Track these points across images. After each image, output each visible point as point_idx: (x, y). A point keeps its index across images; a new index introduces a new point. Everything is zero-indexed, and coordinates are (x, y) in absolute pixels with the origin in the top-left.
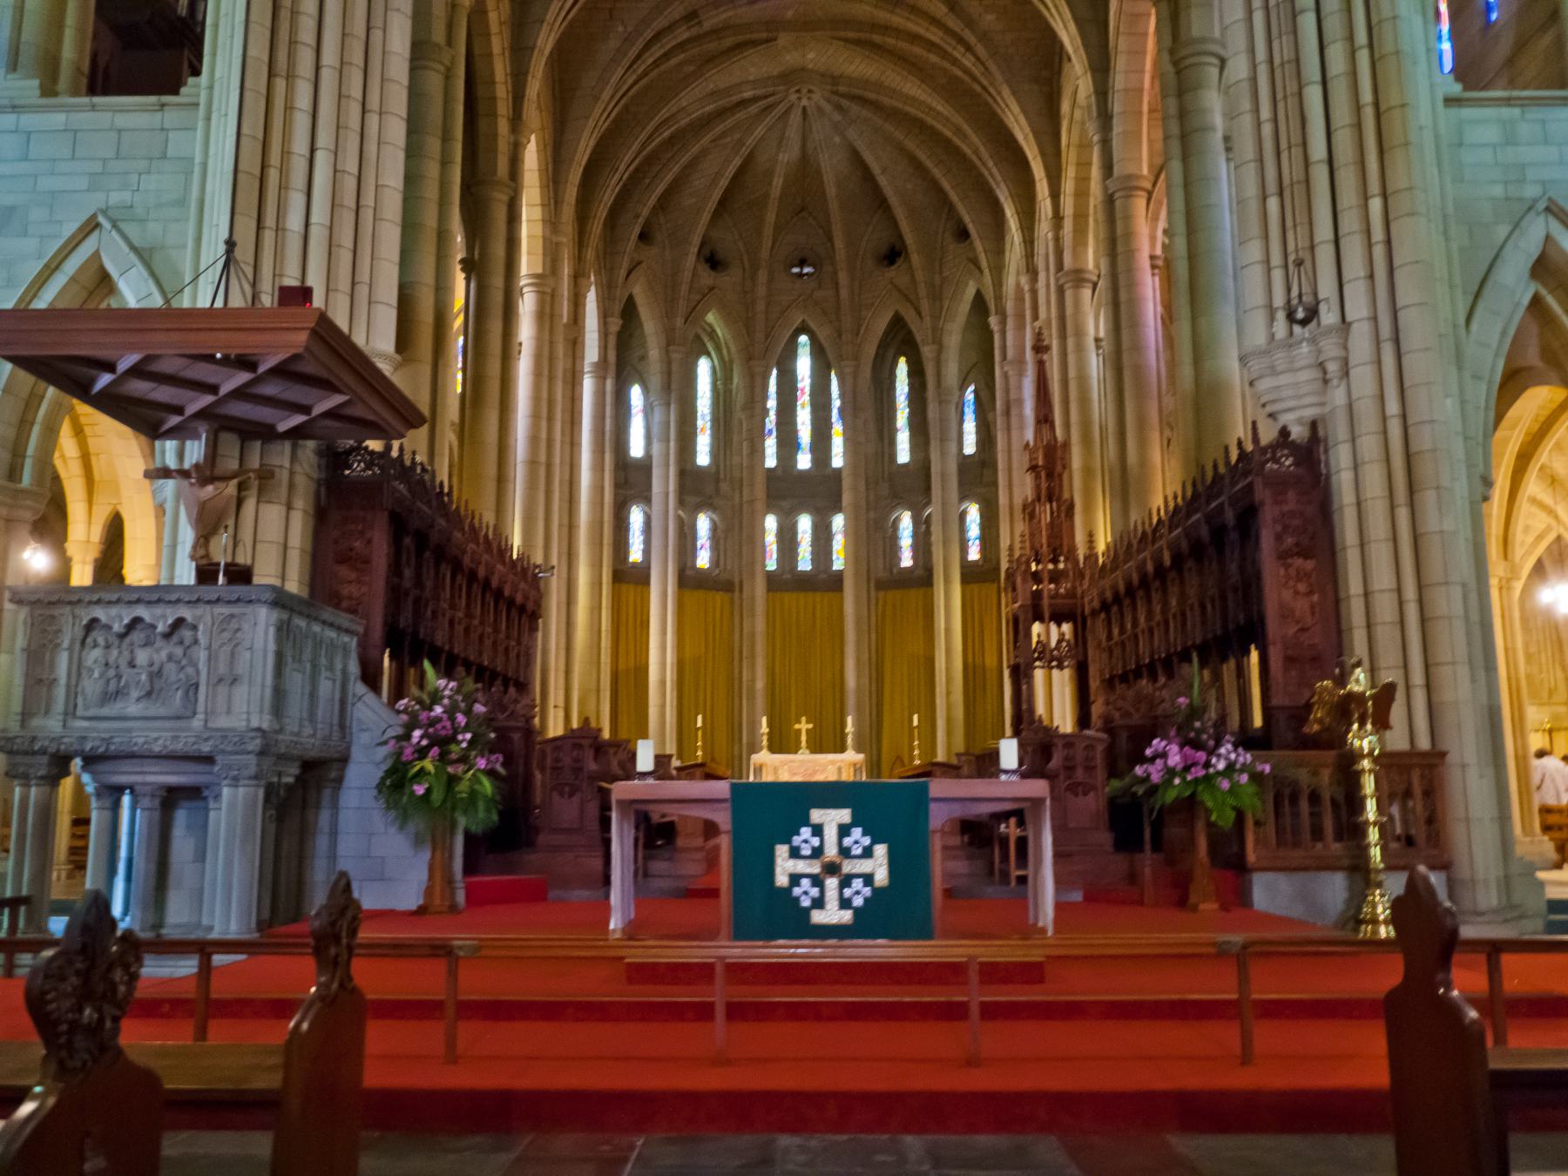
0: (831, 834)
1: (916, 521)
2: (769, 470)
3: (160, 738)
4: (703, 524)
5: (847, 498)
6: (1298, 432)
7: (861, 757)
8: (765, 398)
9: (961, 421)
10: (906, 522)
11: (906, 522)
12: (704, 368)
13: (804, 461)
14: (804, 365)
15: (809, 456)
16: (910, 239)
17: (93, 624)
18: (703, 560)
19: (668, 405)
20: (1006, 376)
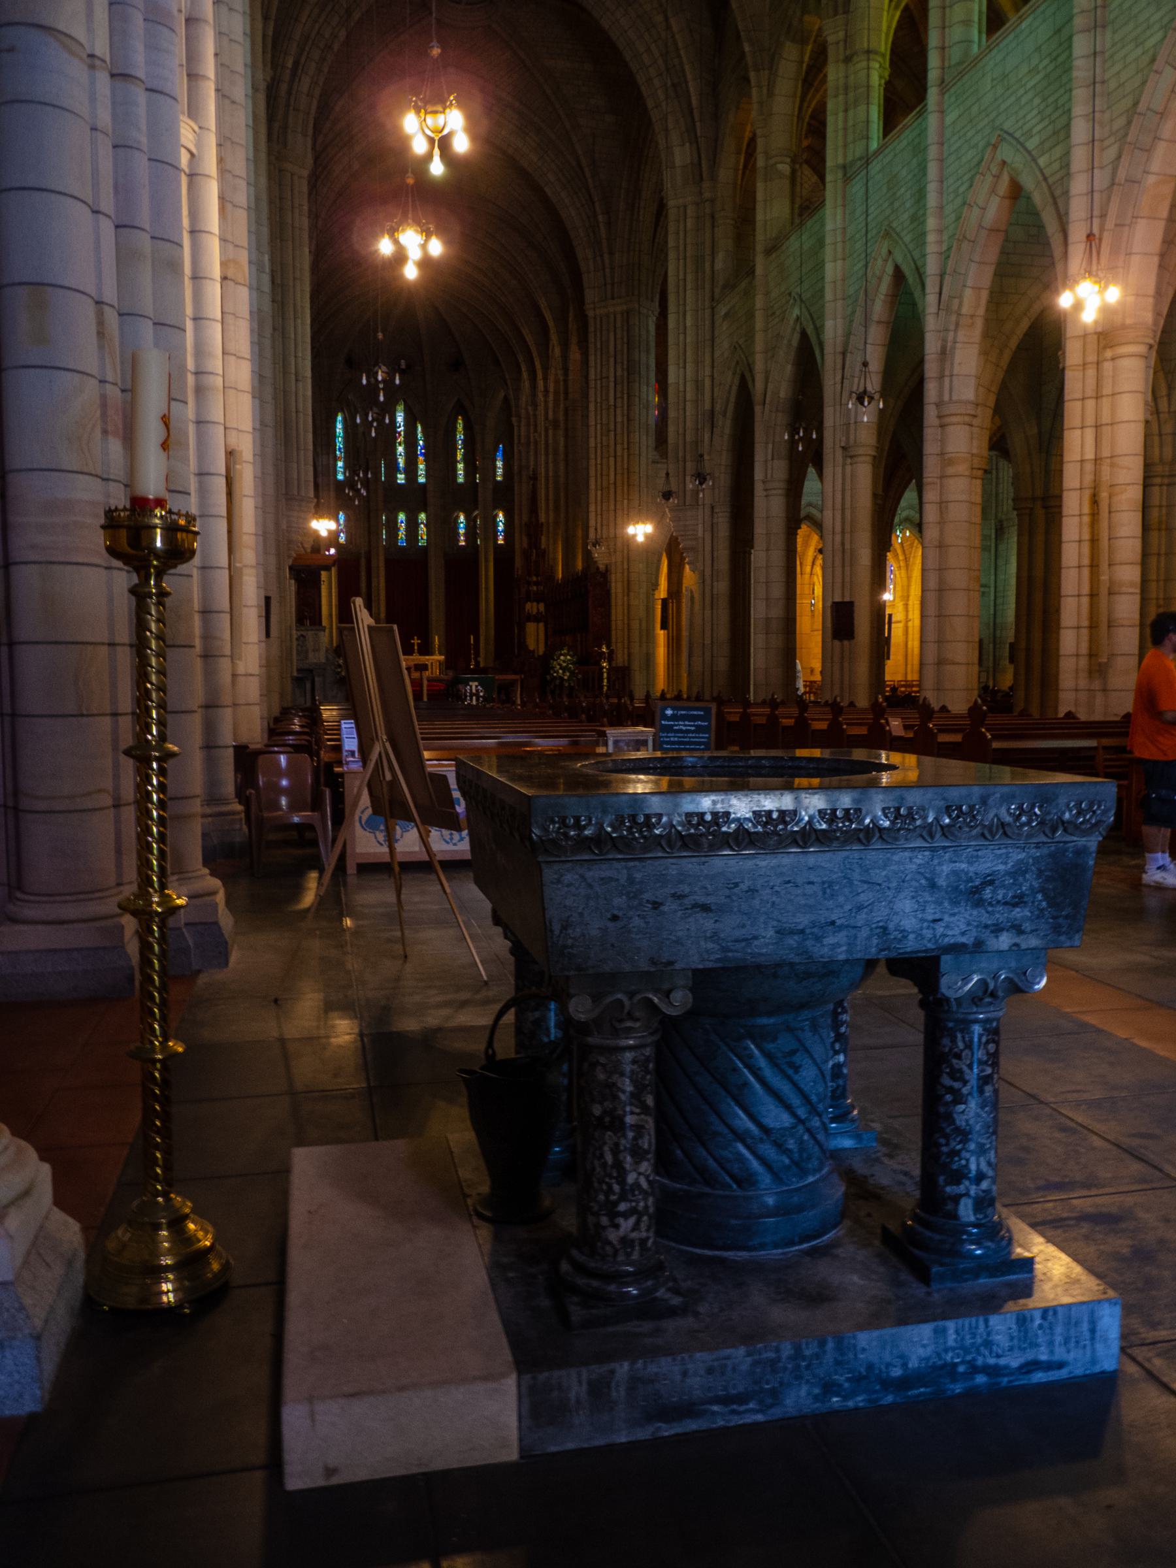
0: (474, 688)
1: (466, 518)
6: (602, 567)
7: (443, 657)
9: (495, 460)
10: (462, 518)
11: (462, 518)
12: (339, 418)
13: (401, 478)
14: (400, 418)
15: (403, 476)
20: (520, 452)
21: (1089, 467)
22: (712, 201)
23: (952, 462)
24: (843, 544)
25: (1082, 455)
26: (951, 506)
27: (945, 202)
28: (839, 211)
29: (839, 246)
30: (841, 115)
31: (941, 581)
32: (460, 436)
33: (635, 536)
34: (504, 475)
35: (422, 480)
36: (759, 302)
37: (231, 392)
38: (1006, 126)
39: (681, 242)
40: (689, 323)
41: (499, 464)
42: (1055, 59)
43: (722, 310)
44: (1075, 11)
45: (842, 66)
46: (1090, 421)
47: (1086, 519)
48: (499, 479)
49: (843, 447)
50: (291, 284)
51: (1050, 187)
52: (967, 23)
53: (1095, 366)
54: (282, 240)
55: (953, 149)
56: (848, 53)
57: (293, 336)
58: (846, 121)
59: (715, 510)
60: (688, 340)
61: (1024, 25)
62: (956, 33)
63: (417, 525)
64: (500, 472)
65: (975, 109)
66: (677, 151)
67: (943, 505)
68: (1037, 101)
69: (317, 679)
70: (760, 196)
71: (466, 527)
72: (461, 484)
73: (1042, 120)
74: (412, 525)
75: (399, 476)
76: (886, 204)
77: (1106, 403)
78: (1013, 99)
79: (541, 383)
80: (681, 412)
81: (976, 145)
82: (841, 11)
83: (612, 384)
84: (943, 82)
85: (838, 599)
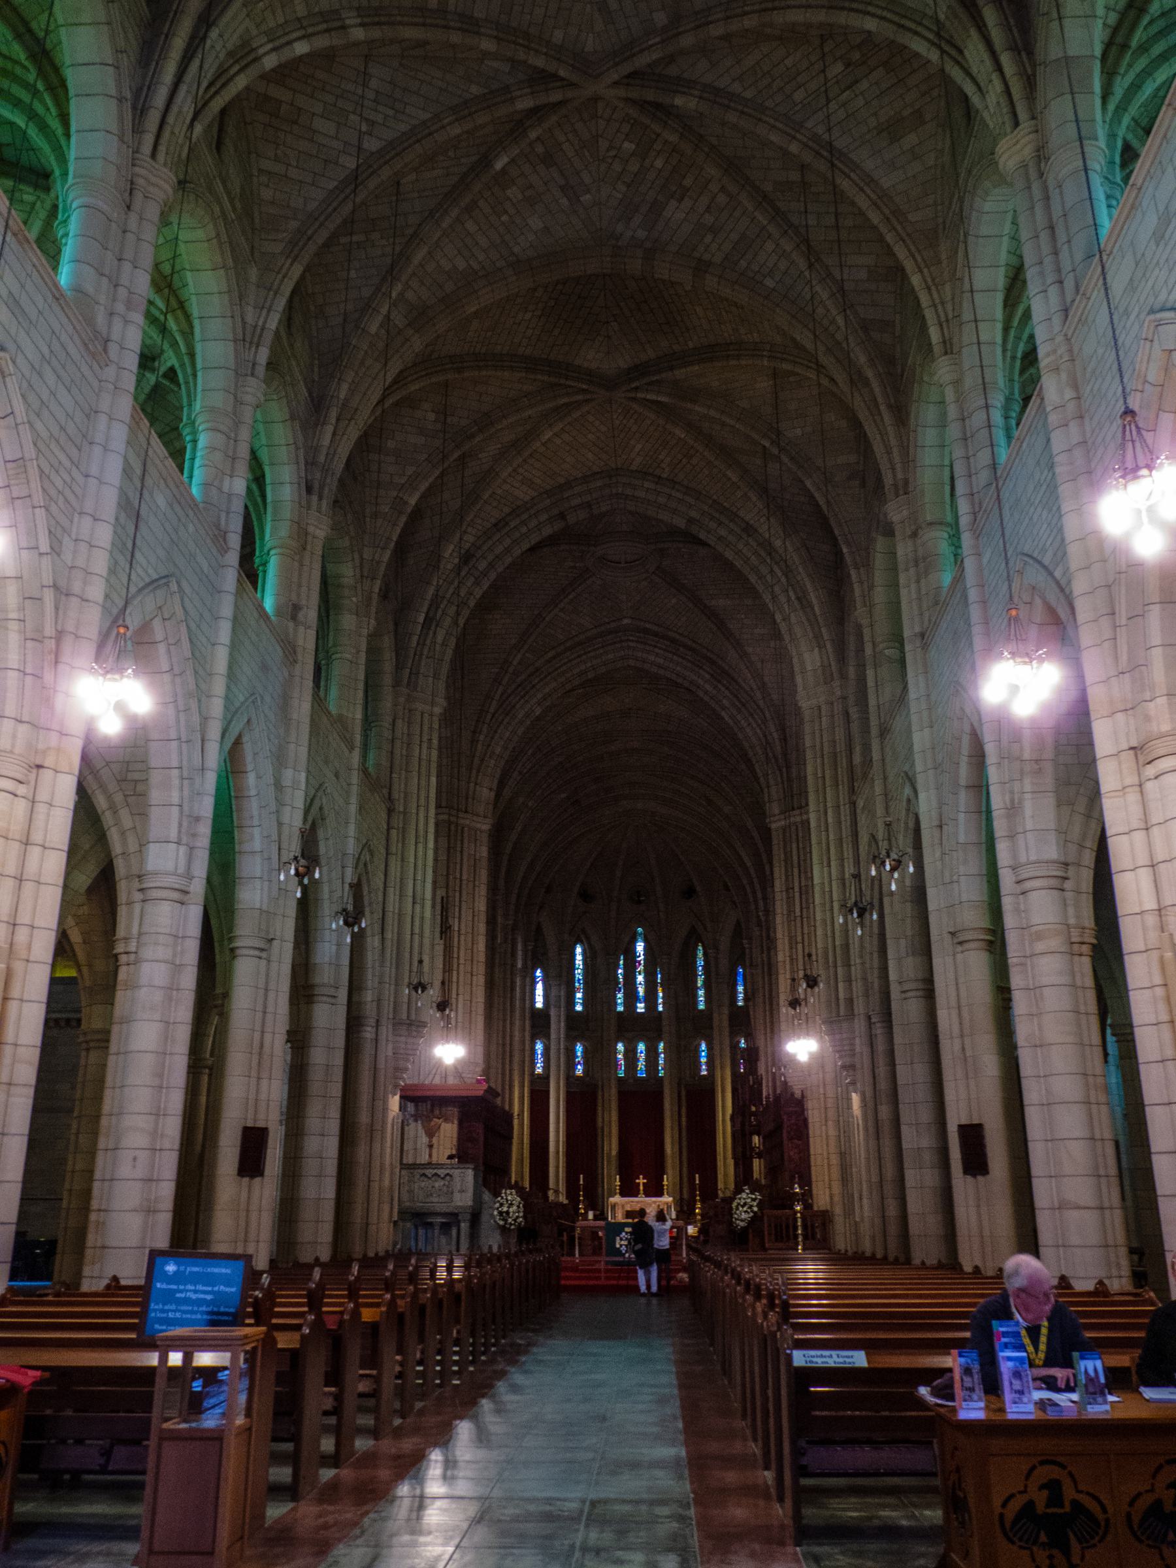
2: (620, 1013)
3: (444, 1208)
4: (579, 1049)
5: (665, 1029)
6: (798, 1094)
8: (618, 967)
9: (735, 985)
10: (703, 1047)
11: (703, 1047)
12: (579, 950)
13: (641, 1007)
14: (640, 947)
15: (642, 1005)
16: (698, 889)
17: (424, 1175)
18: (579, 1070)
19: (560, 985)
21: (1151, 920)
22: (844, 698)
23: (1039, 937)
24: (963, 1049)
25: (1141, 904)
26: (1046, 991)
28: (921, 678)
29: (925, 714)
30: (913, 586)
32: (700, 962)
34: (746, 999)
35: (660, 1008)
36: (878, 789)
37: (28, 887)
38: (1026, 549)
39: (818, 740)
40: (830, 820)
41: (740, 989)
43: (860, 803)
44: (1048, 409)
45: (910, 543)
46: (1143, 859)
47: (1160, 991)
48: (740, 1004)
49: (953, 934)
50: (414, 811)
53: (1138, 789)
54: (407, 771)
56: (913, 527)
57: (412, 860)
58: (919, 590)
59: (873, 1020)
60: (832, 837)
61: (1025, 445)
63: (657, 1054)
64: (741, 996)
66: (806, 656)
67: (1034, 989)
68: (1045, 512)
69: (463, 1225)
70: (870, 683)
71: (709, 1056)
72: (702, 1011)
74: (652, 1054)
75: (639, 1005)
77: (1155, 831)
78: (1027, 520)
79: (761, 903)
80: (828, 914)
82: (901, 492)
83: (797, 895)
85: (964, 1122)
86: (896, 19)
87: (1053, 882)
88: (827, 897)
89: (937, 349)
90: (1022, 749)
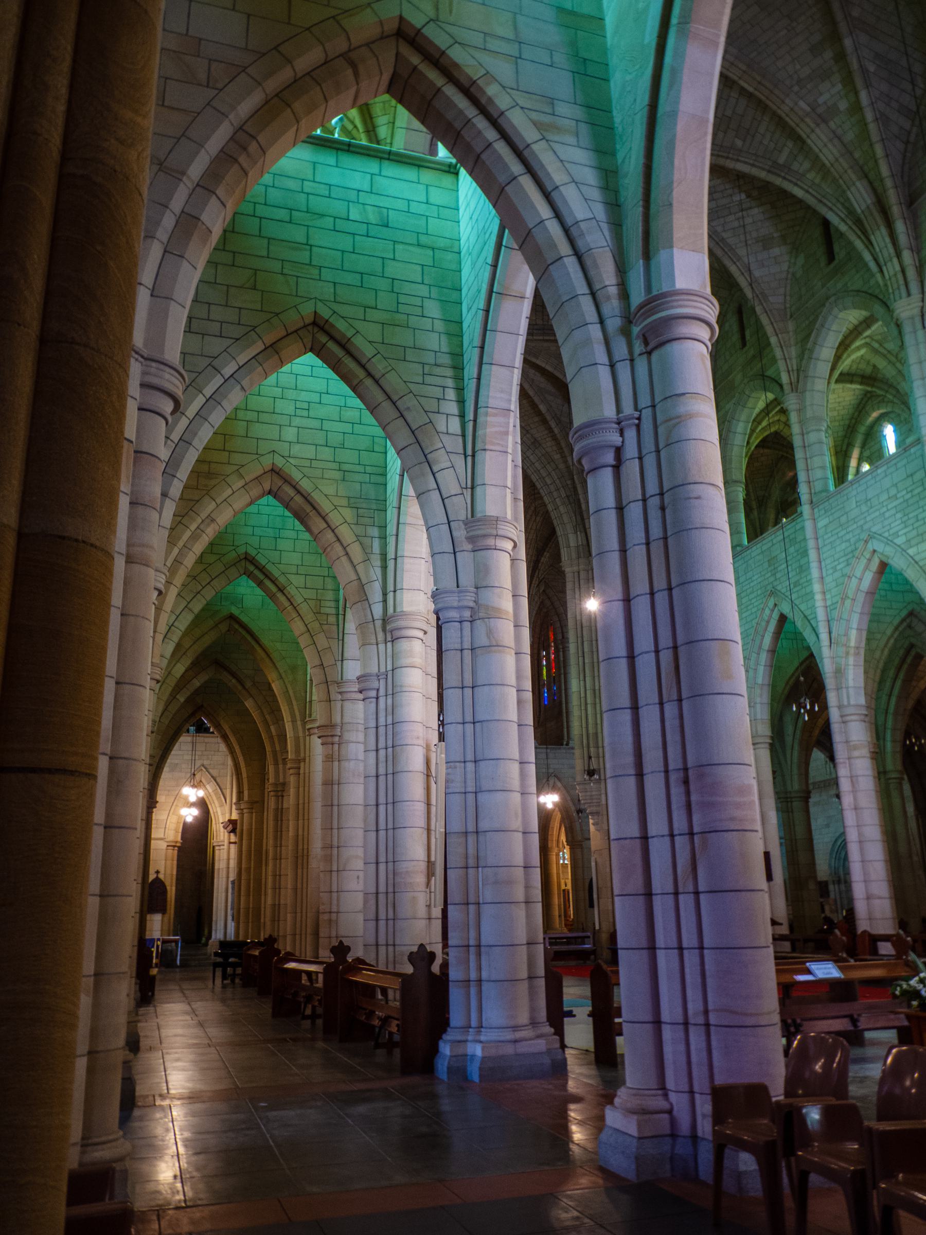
23: (855, 748)
26: (860, 779)
27: (824, 575)
31: (860, 834)
33: (545, 804)
40: (586, 650)
42: (911, 491)
51: (921, 567)
52: (823, 468)
55: (827, 542)
60: (586, 661)
62: (818, 474)
65: (844, 519)
66: (572, 538)
67: (853, 778)
68: (899, 515)
73: (906, 527)
76: (769, 574)
80: (583, 712)
81: (849, 540)
84: (812, 502)
86: (819, 197)
87: (863, 717)
88: (583, 700)
89: (787, 388)
90: (849, 640)
